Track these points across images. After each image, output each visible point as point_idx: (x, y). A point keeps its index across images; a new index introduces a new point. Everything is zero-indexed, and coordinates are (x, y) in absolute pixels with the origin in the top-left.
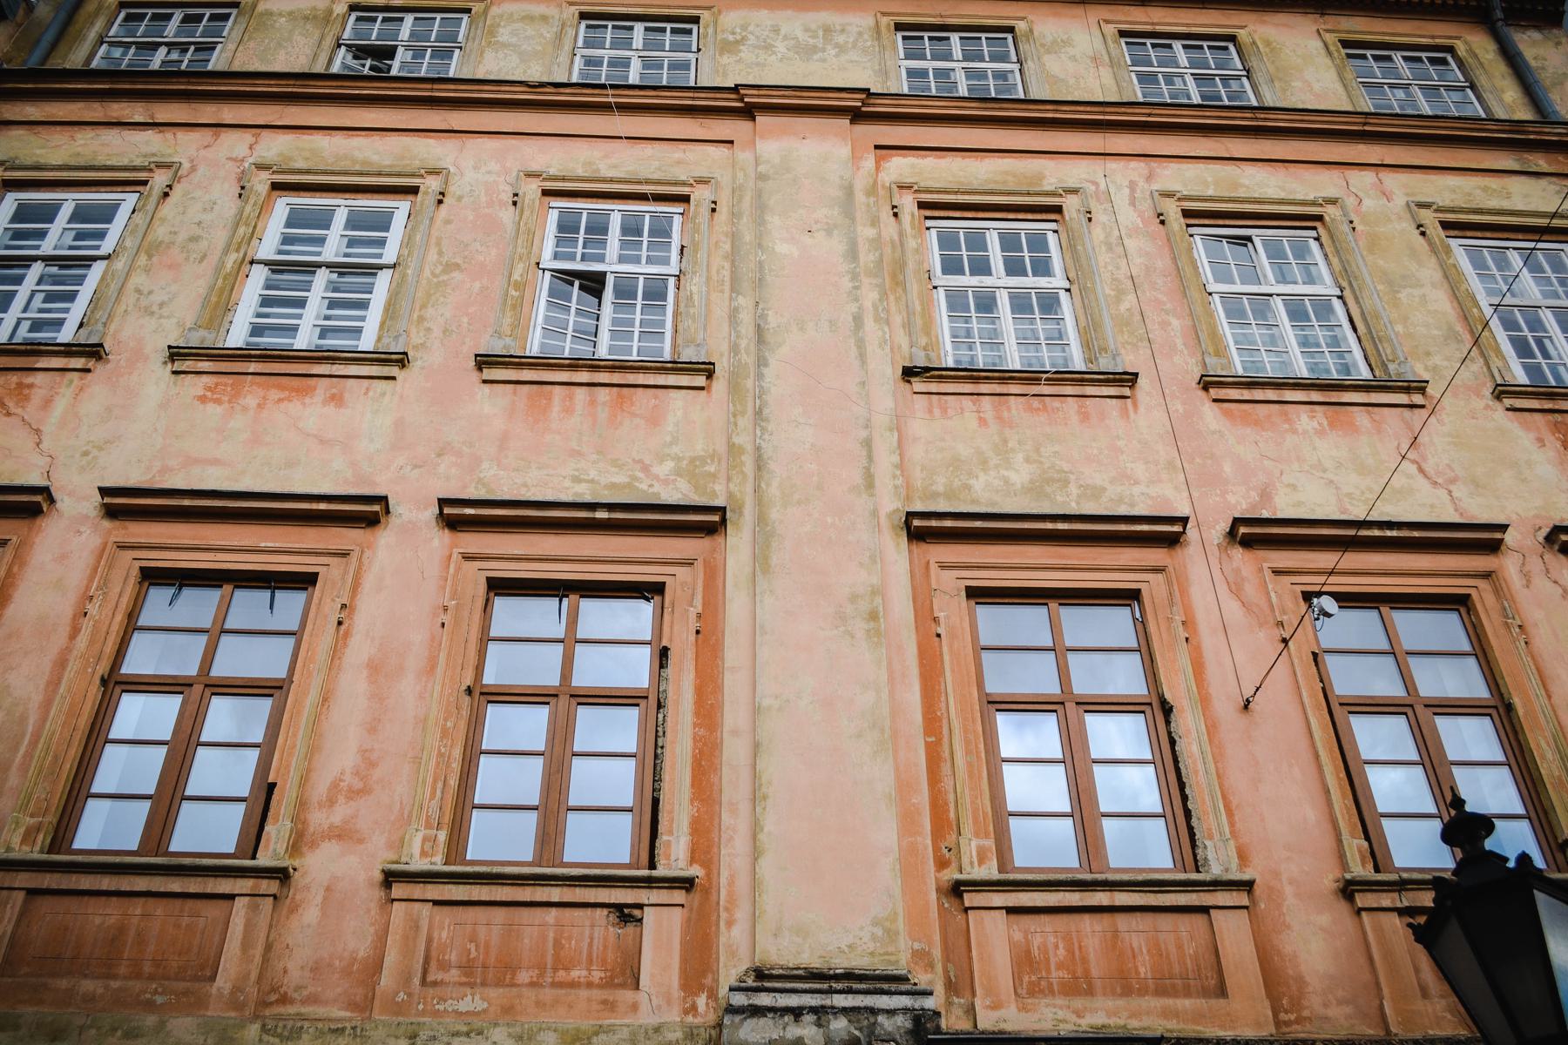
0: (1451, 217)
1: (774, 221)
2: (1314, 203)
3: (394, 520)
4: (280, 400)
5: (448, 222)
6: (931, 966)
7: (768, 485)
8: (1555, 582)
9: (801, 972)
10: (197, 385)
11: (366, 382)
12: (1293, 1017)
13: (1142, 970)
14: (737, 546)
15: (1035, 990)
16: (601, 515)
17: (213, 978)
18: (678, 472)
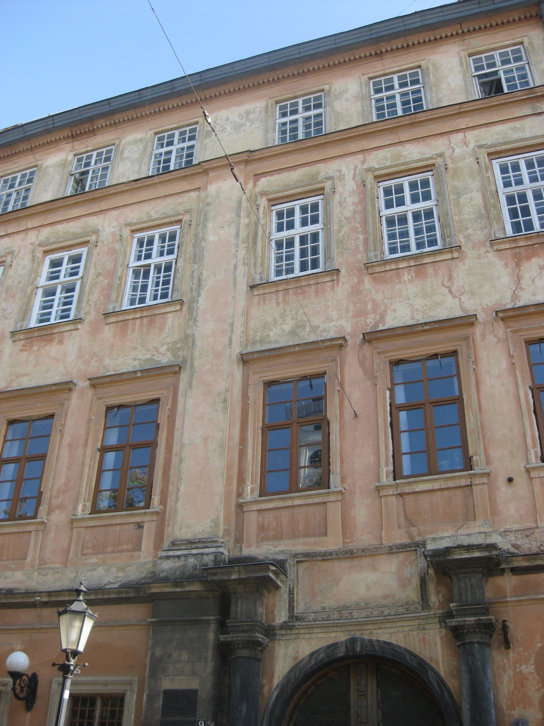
0: (493, 150)
1: (210, 225)
2: (431, 158)
3: (78, 388)
4: (44, 346)
5: (98, 254)
6: (229, 534)
7: (195, 351)
8: (495, 336)
9: (185, 542)
10: (19, 345)
11: (70, 333)
12: (349, 540)
13: (300, 528)
14: (184, 376)
15: (263, 539)
16: (139, 375)
17: (26, 559)
18: (168, 350)
